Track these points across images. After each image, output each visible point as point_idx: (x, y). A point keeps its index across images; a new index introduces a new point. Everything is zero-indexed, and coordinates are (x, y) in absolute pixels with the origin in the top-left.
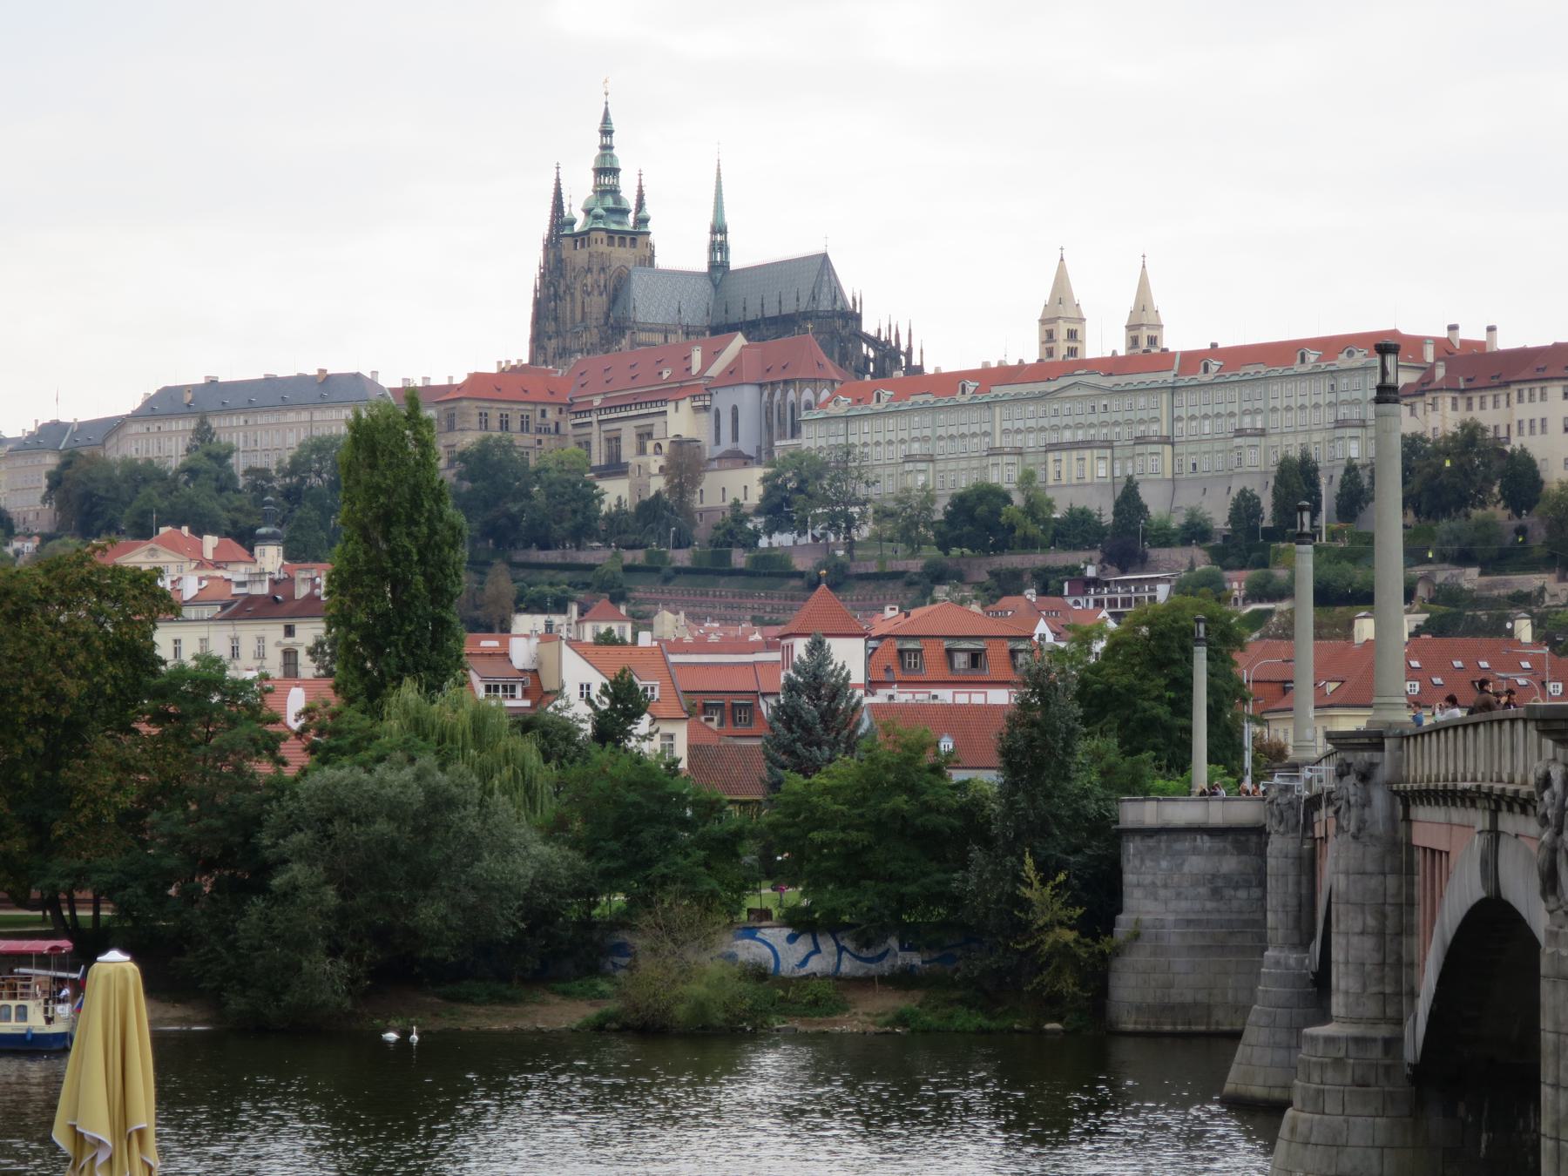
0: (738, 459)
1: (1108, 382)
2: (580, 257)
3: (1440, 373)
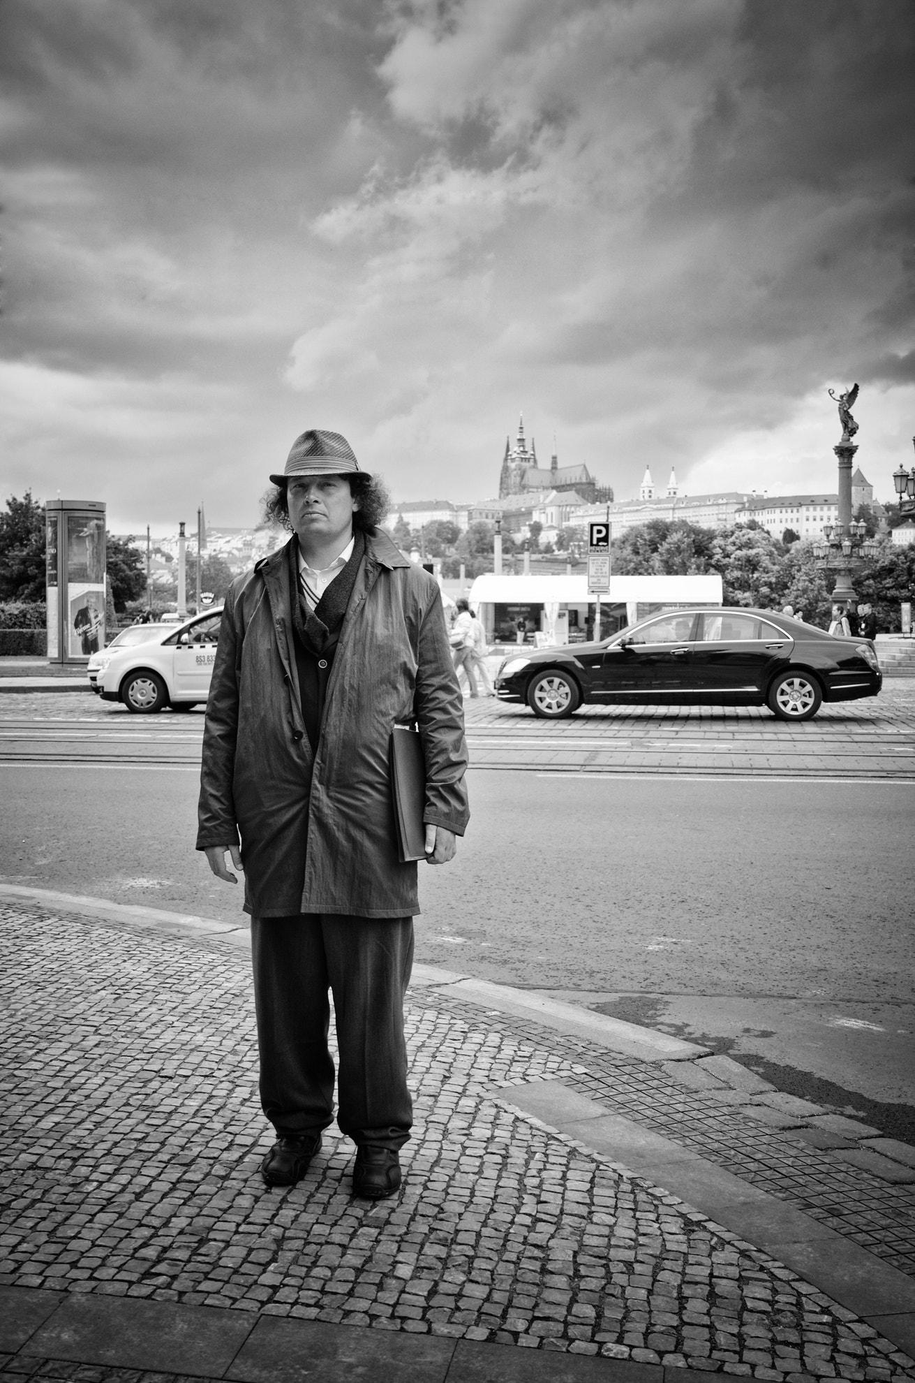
0: (552, 527)
1: (655, 507)
2: (513, 465)
3: (747, 505)
